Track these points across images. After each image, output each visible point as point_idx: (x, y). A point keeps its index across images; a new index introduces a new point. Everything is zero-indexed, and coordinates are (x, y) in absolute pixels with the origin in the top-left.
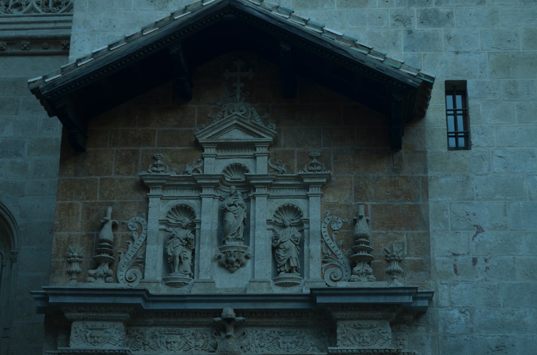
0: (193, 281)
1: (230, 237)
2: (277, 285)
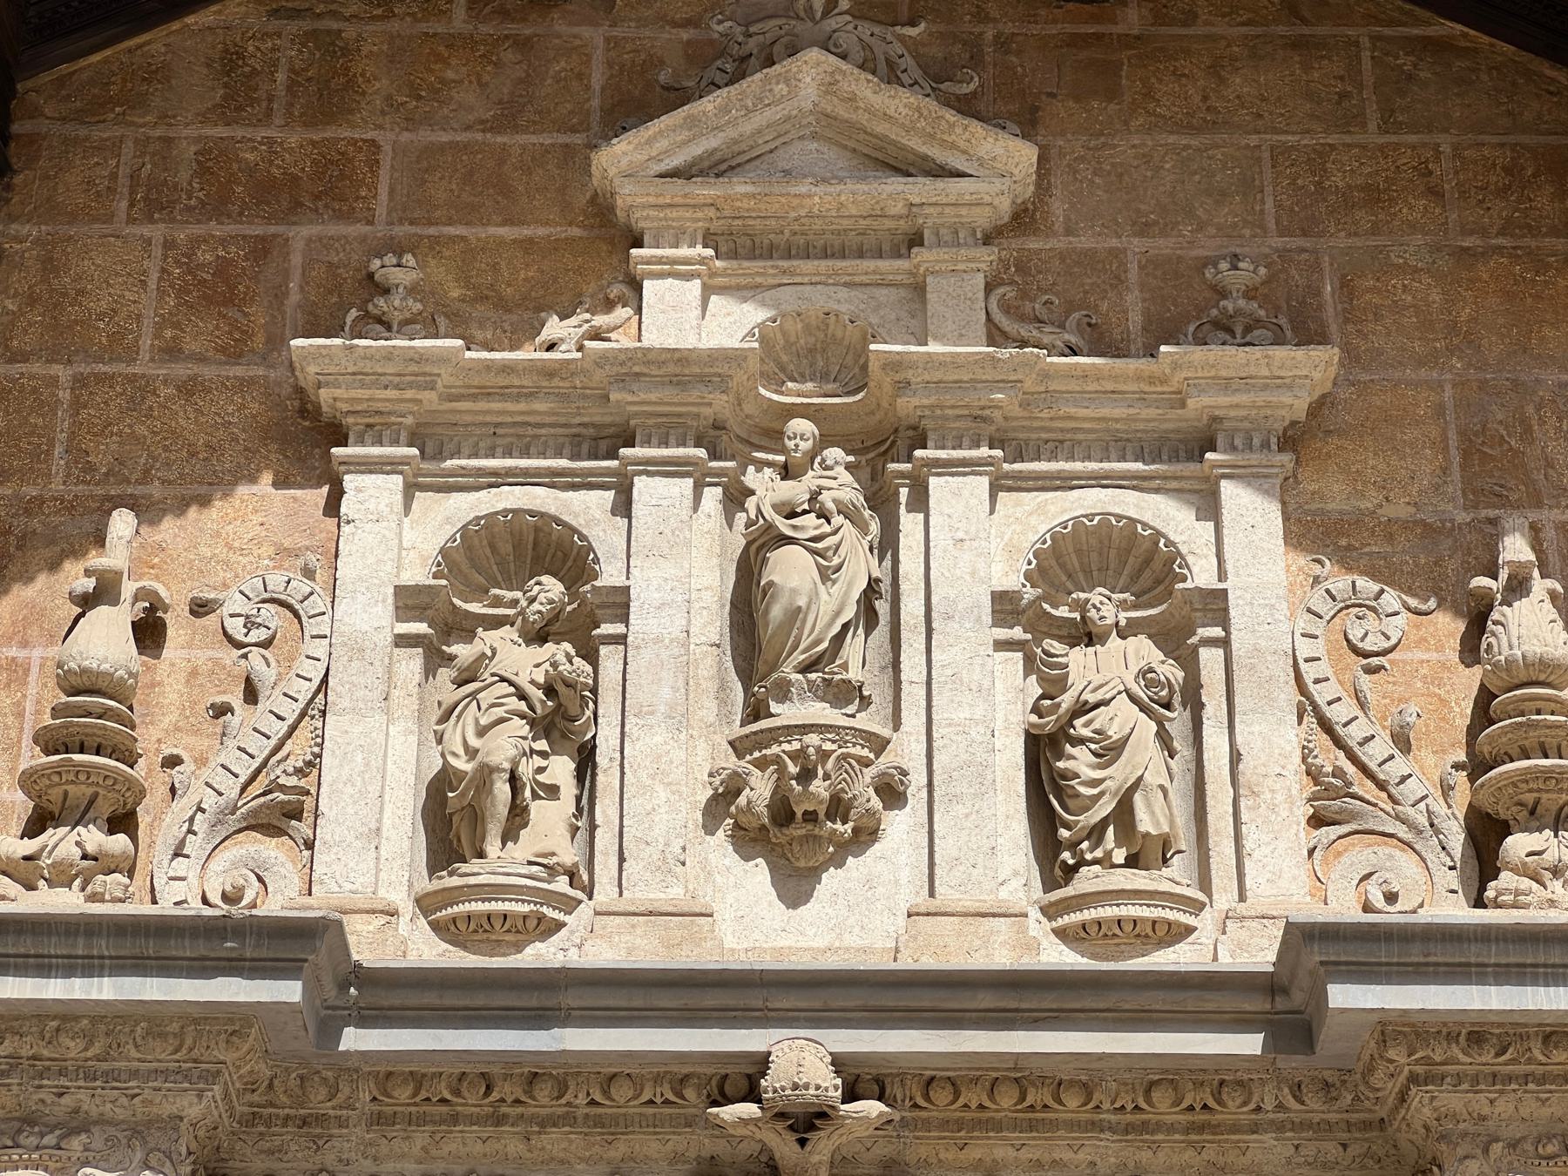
0: (586, 909)
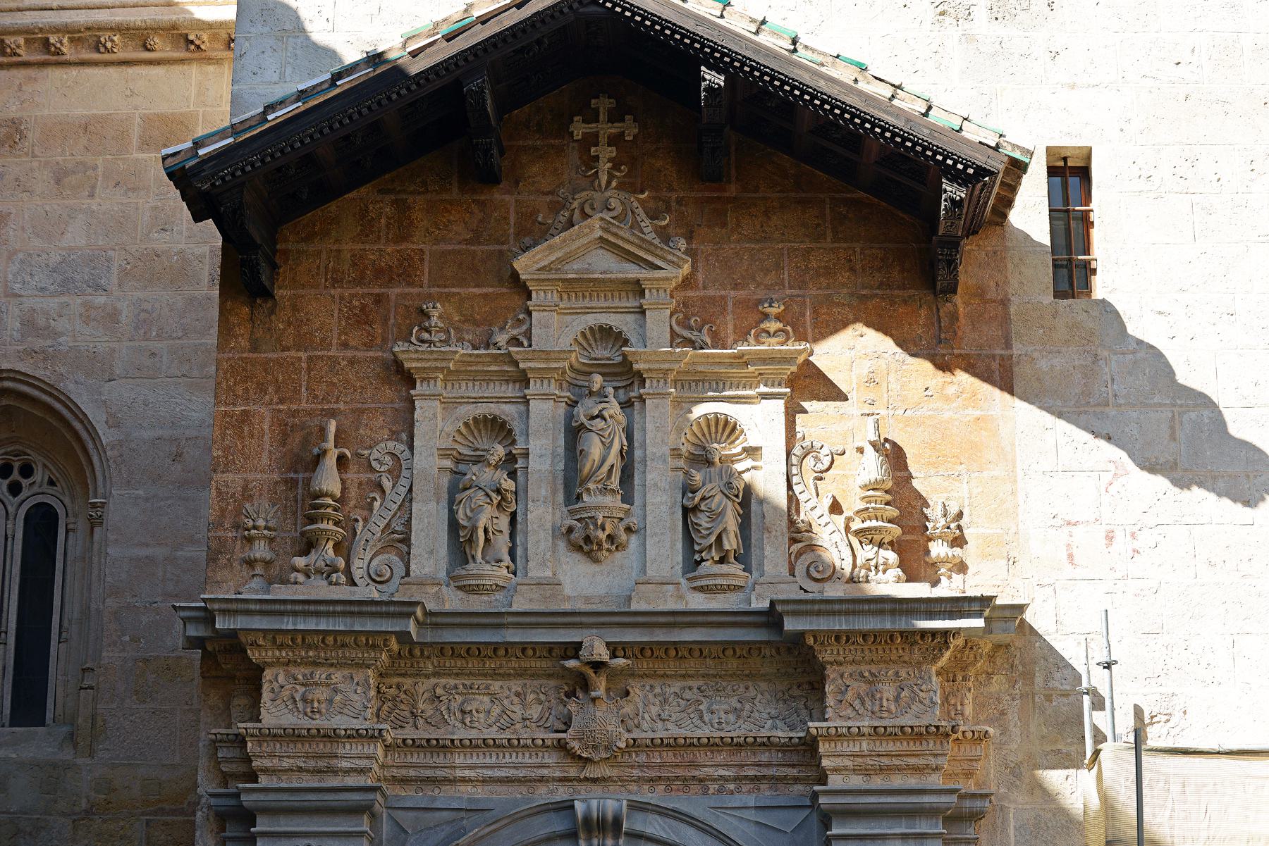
2: (694, 588)
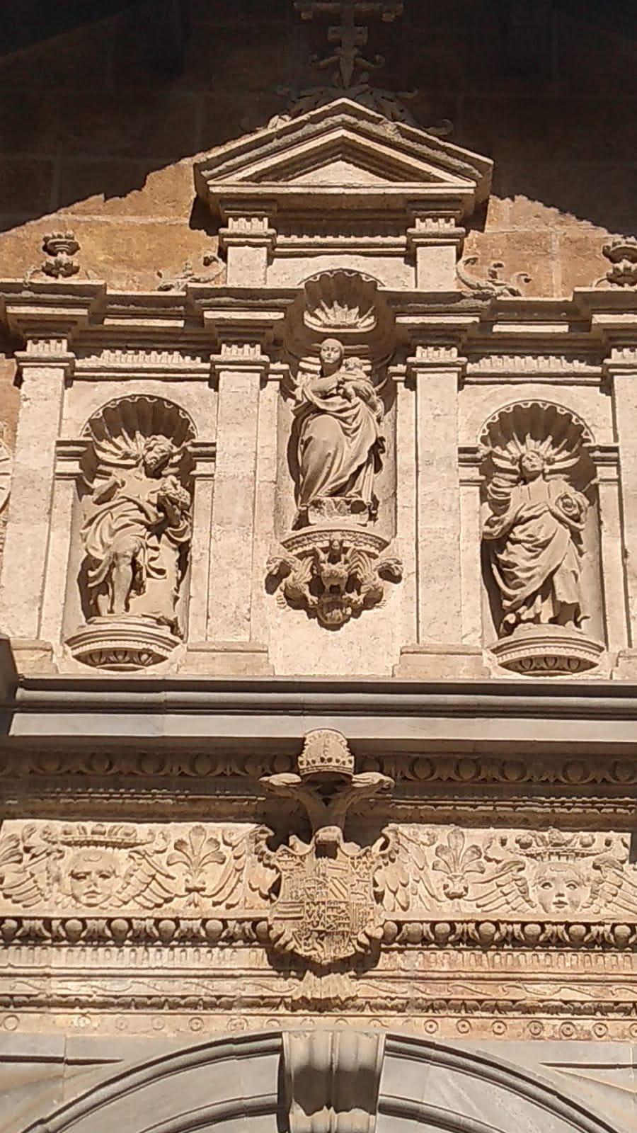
0: (180, 649)
1: (326, 499)
2: (506, 666)
